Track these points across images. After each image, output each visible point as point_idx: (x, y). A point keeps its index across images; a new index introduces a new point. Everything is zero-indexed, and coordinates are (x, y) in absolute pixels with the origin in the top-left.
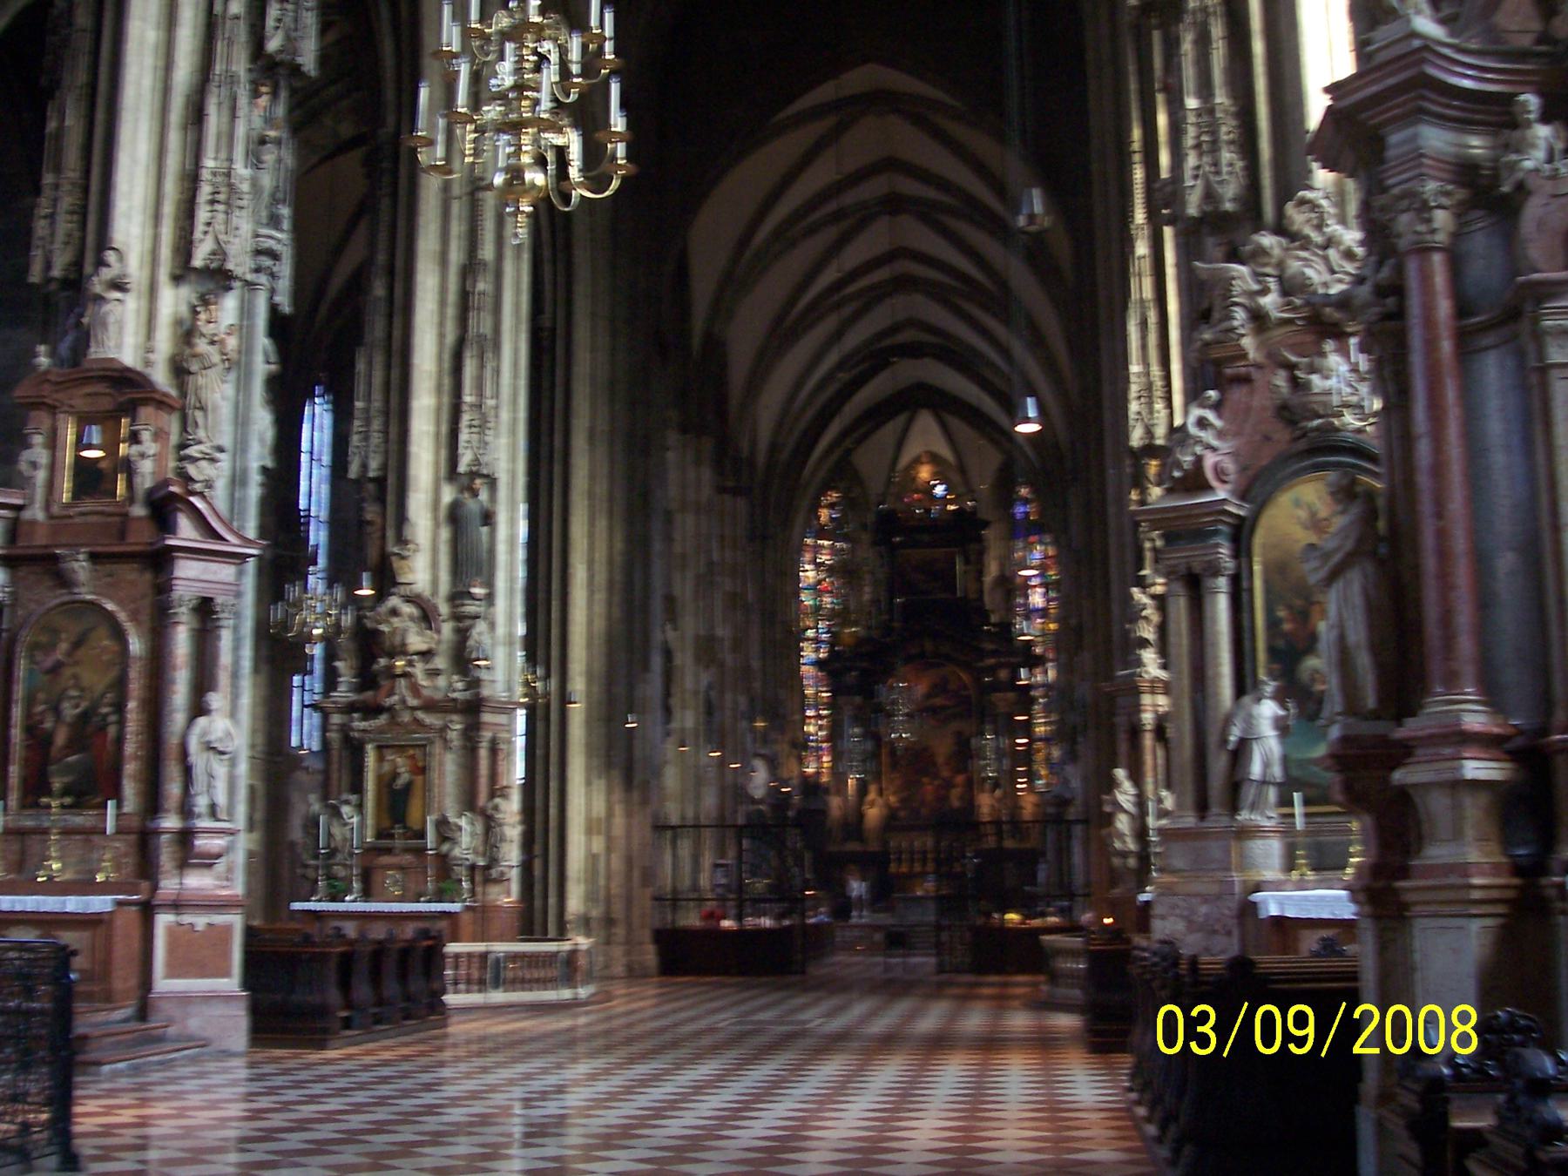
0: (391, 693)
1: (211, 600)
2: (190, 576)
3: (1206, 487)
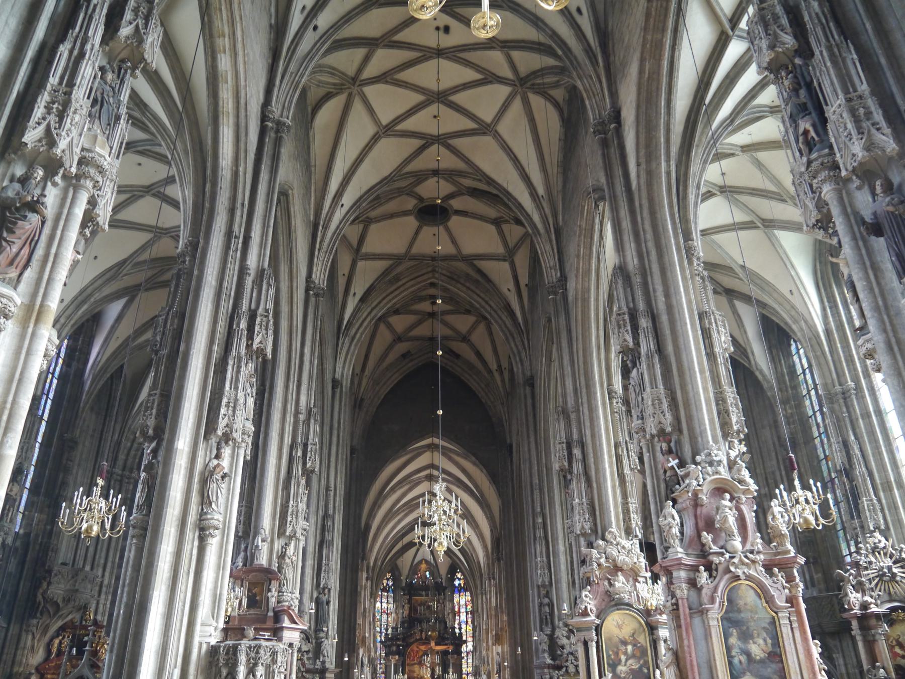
3: (588, 615)
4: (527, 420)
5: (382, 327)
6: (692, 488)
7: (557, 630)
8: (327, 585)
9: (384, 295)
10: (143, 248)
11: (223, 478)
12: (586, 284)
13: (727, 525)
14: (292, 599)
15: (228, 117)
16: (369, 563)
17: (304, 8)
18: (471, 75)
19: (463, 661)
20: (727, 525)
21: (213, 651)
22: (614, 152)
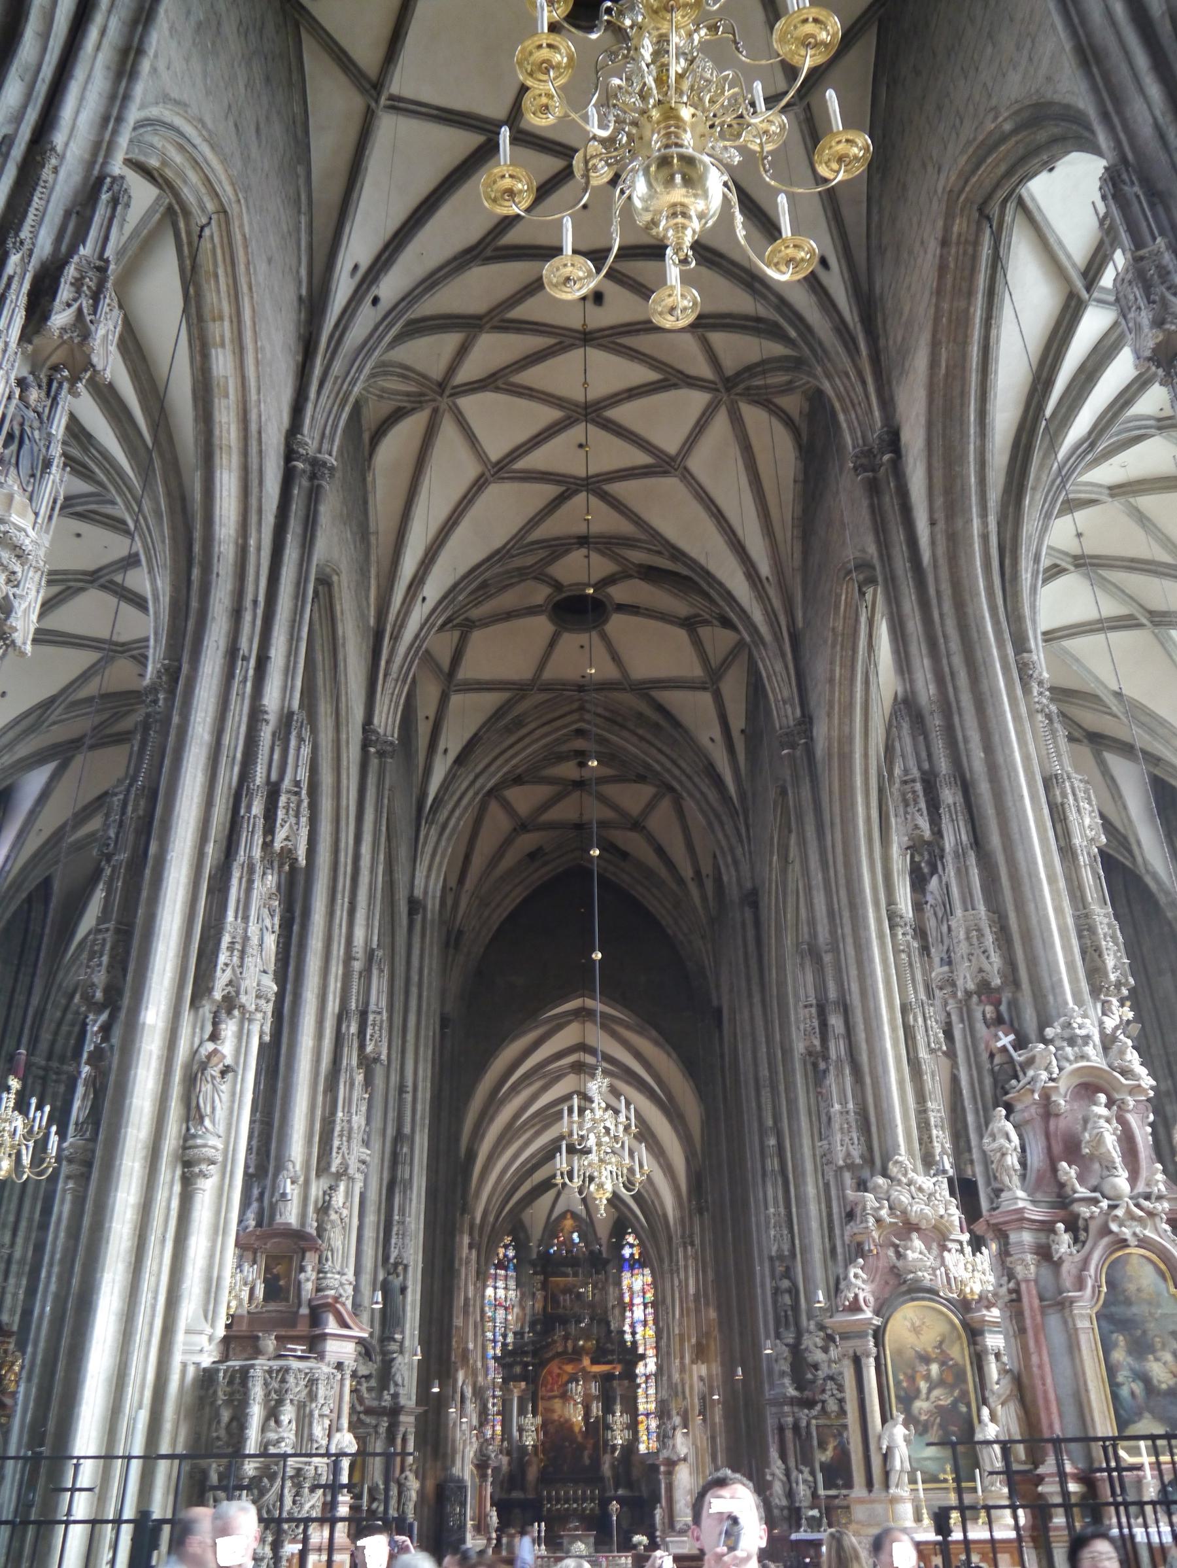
3: (859, 1310)
4: (747, 966)
5: (494, 807)
6: (1040, 1085)
7: (806, 1336)
9: (497, 751)
10: (85, 677)
11: (223, 1073)
12: (847, 729)
13: (1103, 1150)
14: (342, 1284)
15: (230, 455)
16: (473, 1219)
17: (356, 267)
18: (642, 374)
19: (640, 1391)
20: (1103, 1150)
21: (207, 1378)
22: (890, 502)
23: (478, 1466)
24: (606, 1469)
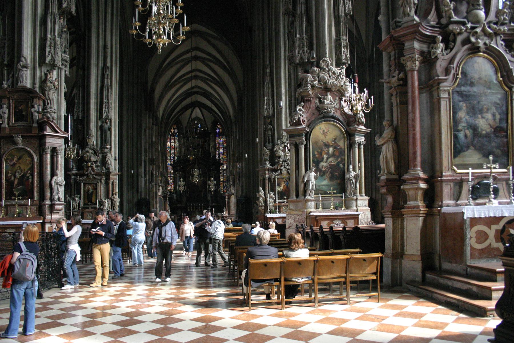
0: (87, 170)
1: (56, 148)
2: (50, 142)
8: (108, 116)
23: (163, 197)
24: (209, 198)
